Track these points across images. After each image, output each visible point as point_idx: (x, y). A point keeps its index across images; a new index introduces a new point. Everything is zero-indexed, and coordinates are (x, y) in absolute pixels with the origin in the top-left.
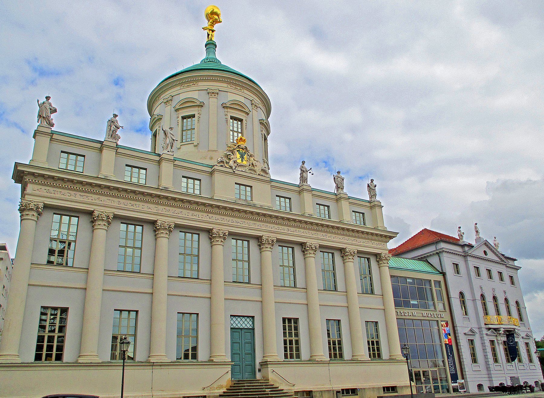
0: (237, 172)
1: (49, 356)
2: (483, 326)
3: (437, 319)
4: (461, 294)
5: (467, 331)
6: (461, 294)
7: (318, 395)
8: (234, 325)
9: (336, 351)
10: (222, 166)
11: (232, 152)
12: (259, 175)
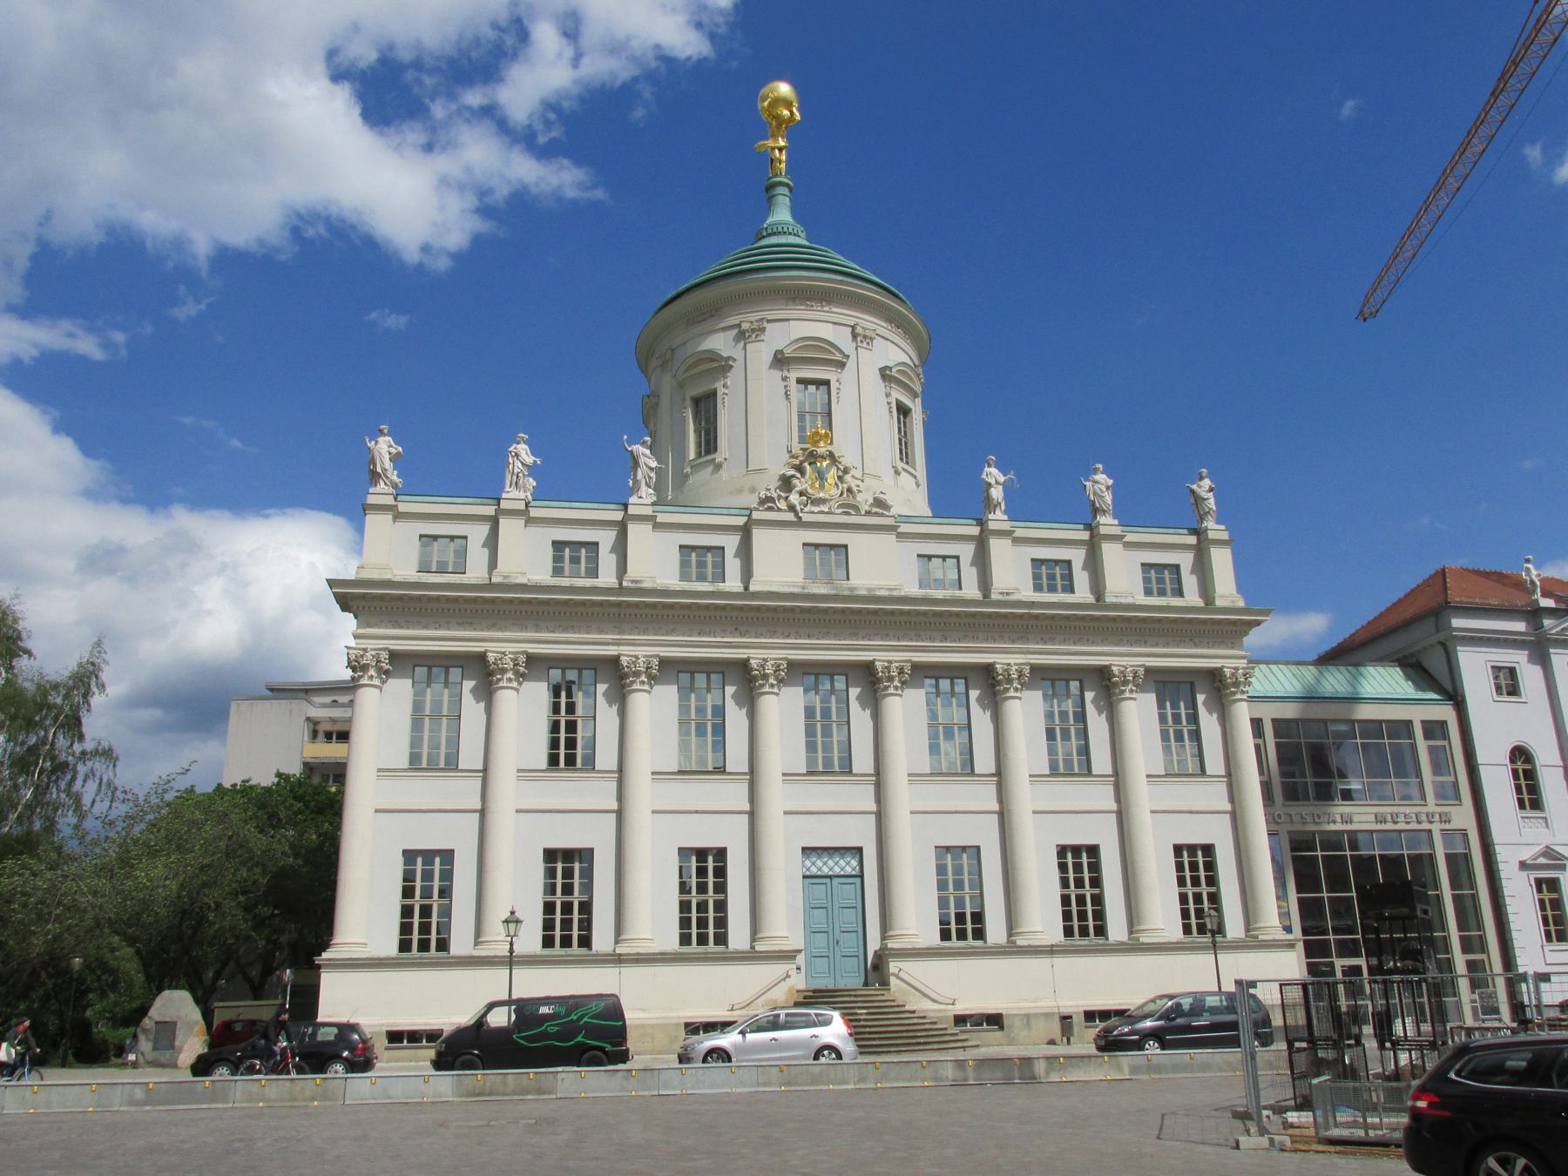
0: (806, 518)
1: (424, 946)
3: (1425, 826)
4: (1520, 754)
5: (1527, 854)
6: (1520, 754)
7: (1017, 1023)
8: (814, 870)
9: (1084, 919)
10: (770, 509)
11: (800, 469)
12: (868, 513)
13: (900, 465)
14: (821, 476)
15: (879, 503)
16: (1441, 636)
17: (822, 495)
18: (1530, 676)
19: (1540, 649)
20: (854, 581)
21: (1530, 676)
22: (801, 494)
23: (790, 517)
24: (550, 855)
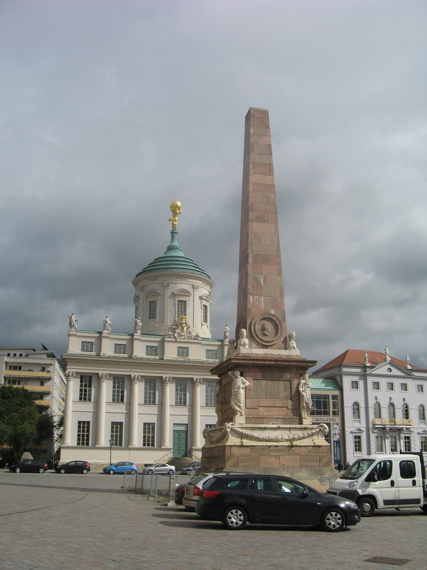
0: (178, 340)
2: (371, 426)
3: (329, 422)
4: (356, 404)
5: (353, 430)
6: (356, 404)
8: (176, 429)
10: (170, 337)
12: (194, 339)
13: (203, 323)
14: (183, 328)
15: (197, 336)
16: (340, 373)
17: (183, 334)
18: (361, 384)
19: (364, 377)
20: (190, 357)
21: (361, 384)
22: (178, 333)
23: (174, 340)
24: (113, 423)
